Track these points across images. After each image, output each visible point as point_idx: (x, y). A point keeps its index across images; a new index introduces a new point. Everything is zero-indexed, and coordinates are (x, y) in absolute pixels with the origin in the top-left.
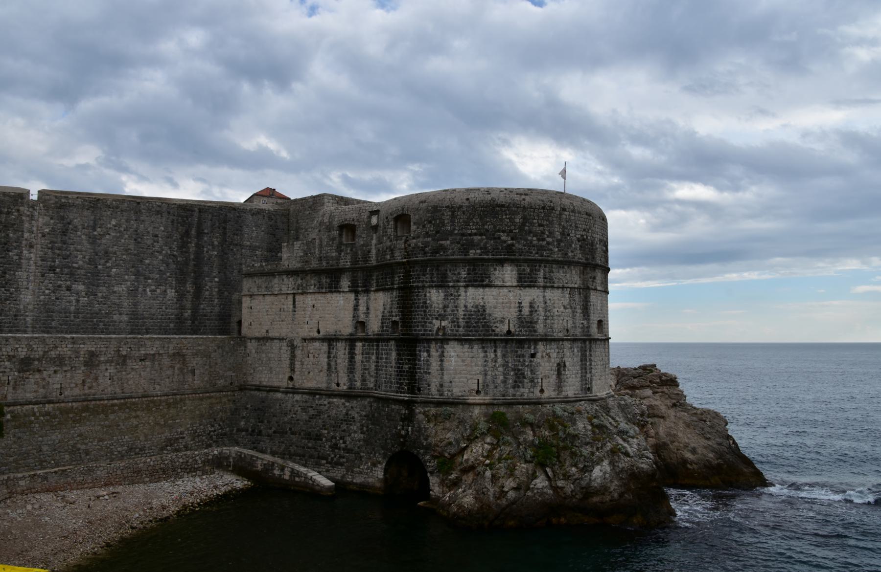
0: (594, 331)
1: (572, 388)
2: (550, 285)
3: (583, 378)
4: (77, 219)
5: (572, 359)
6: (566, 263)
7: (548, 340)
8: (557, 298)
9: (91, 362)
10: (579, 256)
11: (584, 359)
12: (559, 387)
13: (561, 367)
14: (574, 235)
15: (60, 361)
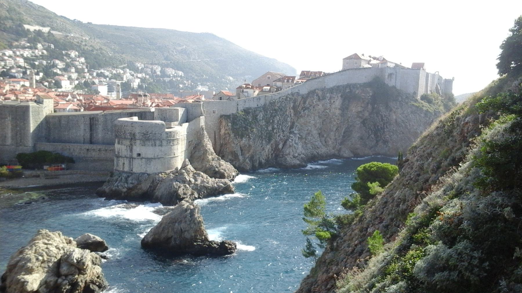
0: (135, 155)
1: (126, 169)
2: (122, 144)
3: (130, 167)
4: (109, 118)
5: (127, 162)
6: (125, 138)
7: (121, 157)
8: (123, 148)
9: (100, 150)
10: (129, 137)
11: (130, 162)
12: (123, 169)
13: (124, 164)
14: (127, 132)
15: (94, 150)
